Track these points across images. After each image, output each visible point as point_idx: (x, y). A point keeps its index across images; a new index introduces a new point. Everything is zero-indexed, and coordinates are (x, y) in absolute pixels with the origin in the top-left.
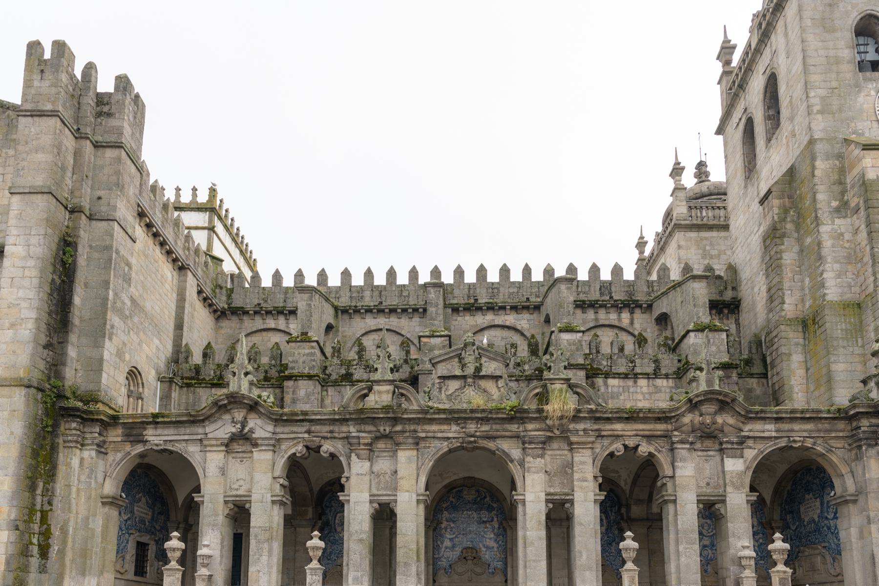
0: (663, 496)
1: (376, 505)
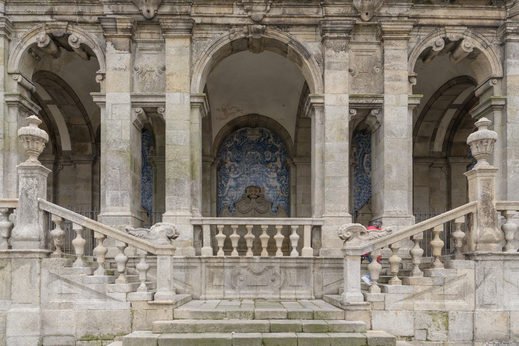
0: (490, 100)
1: (140, 110)
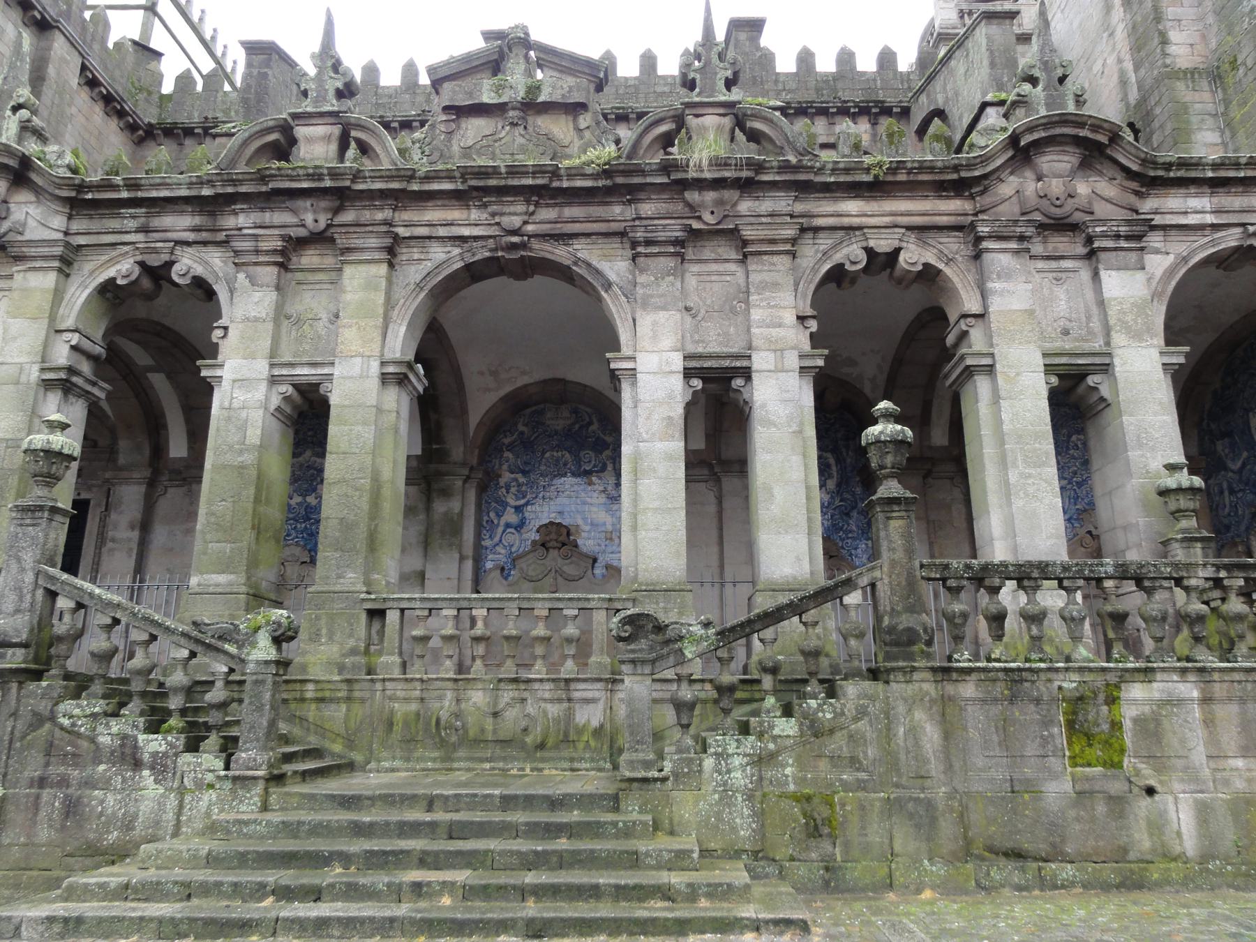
0: (962, 358)
